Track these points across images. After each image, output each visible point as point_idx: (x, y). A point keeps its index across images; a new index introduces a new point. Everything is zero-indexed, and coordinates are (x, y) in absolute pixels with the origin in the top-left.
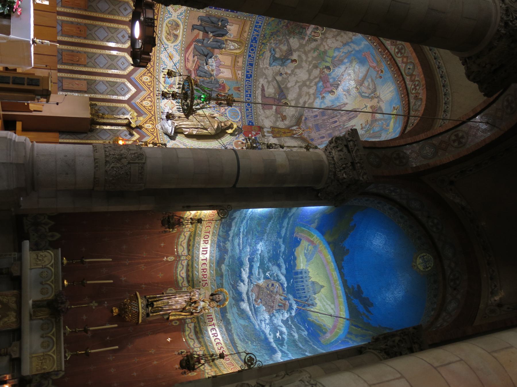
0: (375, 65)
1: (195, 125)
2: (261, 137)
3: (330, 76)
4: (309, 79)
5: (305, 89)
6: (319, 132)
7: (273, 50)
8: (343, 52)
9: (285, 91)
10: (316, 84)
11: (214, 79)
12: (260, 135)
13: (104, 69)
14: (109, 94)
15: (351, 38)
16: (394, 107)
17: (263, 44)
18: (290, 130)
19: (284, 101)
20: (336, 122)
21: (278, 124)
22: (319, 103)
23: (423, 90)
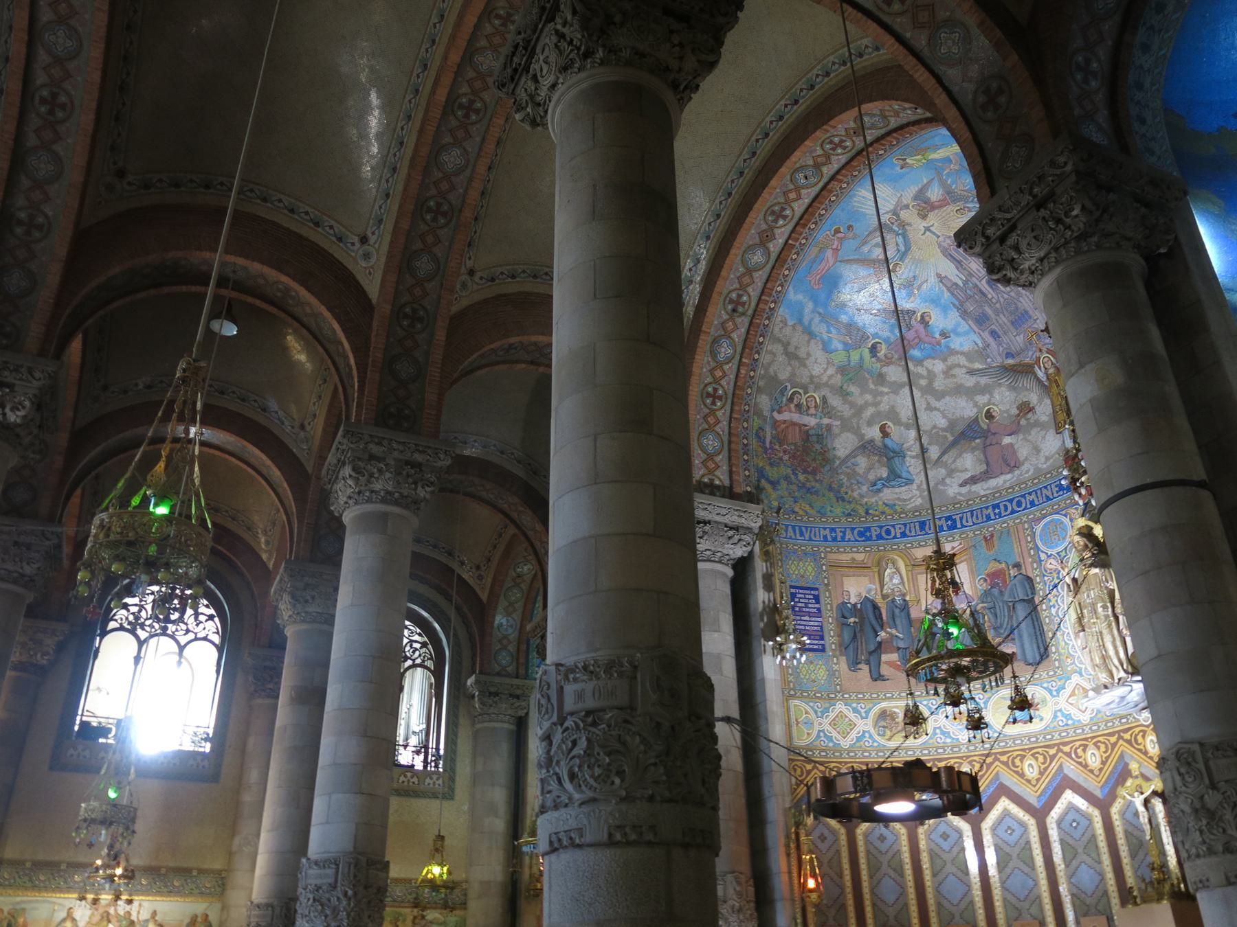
0: (829, 253)
1: (1110, 625)
3: (889, 338)
5: (939, 384)
6: (1031, 312)
8: (829, 332)
9: (960, 428)
11: (983, 602)
13: (1037, 875)
14: (1094, 855)
15: (793, 326)
16: (902, 168)
17: (867, 513)
18: (1050, 384)
19: (984, 423)
21: (1044, 418)
22: (961, 339)
23: (834, 127)
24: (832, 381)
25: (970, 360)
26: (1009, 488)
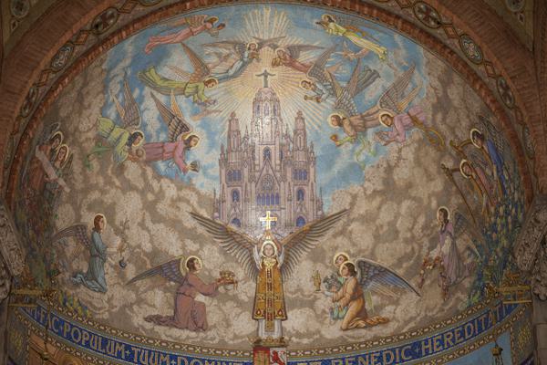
0: (187, 30)
2: (284, 349)
4: (143, 193)
5: (162, 208)
6: (282, 200)
7: (75, 277)
9: (161, 261)
10: (158, 177)
12: (280, 351)
17: (64, 304)
19: (184, 270)
20: (267, 151)
21: (244, 297)
24: (85, 145)
25: (199, 203)
26: (191, 346)
